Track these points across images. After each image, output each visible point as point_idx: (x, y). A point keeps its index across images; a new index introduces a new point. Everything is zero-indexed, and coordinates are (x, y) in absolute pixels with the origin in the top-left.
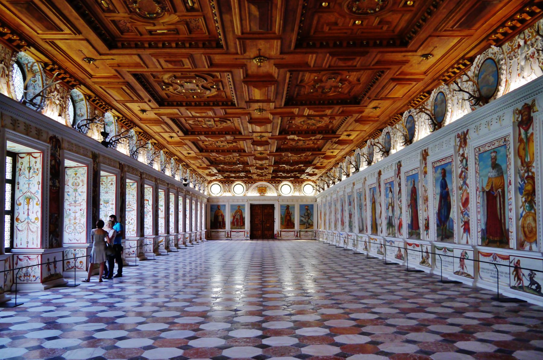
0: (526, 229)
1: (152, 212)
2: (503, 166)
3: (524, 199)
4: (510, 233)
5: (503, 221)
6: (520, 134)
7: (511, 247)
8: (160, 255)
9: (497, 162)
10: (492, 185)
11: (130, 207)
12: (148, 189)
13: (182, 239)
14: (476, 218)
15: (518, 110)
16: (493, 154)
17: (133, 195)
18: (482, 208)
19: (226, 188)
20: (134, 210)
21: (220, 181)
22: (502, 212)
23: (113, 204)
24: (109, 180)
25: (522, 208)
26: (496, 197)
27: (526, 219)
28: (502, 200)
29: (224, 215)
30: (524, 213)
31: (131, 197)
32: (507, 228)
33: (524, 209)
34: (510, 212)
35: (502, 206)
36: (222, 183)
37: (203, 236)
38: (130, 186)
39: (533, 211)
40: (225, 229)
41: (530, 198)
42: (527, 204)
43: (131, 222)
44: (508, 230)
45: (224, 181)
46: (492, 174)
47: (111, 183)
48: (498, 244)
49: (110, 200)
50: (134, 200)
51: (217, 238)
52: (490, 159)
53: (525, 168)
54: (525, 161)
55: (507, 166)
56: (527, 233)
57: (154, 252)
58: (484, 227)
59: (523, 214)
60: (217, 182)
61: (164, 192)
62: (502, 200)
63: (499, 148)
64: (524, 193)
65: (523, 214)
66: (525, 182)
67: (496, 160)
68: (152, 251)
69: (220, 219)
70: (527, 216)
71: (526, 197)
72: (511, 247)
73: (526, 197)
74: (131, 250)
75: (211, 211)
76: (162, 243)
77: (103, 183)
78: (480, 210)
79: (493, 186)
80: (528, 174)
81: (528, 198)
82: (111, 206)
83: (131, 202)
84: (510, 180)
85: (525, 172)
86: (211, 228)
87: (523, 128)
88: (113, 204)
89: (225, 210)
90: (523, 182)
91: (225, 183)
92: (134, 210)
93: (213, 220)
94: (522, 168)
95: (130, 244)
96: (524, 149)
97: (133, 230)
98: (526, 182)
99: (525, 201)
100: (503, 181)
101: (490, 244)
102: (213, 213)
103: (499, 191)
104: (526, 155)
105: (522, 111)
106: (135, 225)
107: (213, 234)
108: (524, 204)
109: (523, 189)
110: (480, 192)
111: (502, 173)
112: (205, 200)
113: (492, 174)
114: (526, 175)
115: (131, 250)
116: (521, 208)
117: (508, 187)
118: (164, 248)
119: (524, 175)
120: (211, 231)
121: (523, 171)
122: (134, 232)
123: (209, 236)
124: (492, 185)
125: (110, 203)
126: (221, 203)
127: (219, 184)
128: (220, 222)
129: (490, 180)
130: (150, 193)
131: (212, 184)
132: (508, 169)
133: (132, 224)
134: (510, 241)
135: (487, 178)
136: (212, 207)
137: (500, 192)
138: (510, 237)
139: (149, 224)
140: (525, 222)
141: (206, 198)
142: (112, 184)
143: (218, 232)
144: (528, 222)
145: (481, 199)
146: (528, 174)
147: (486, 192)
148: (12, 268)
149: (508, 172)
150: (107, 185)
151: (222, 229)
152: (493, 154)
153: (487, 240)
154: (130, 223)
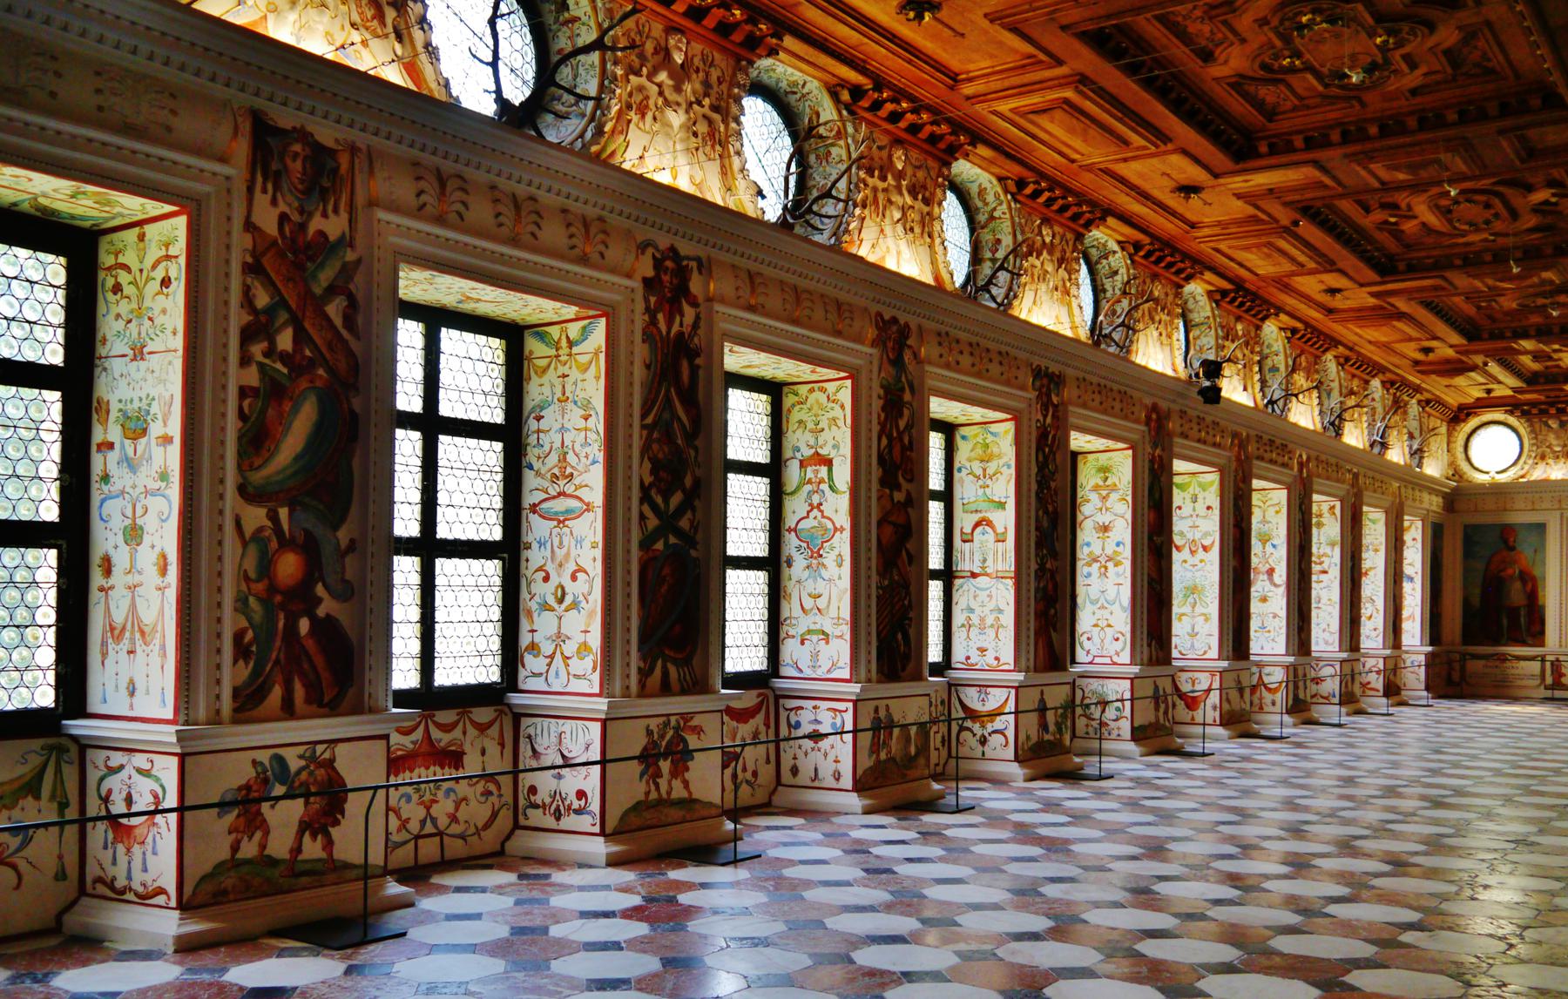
1: (847, 535)
8: (1256, 736)
11: (570, 489)
12: (831, 387)
13: (1214, 698)
17: (587, 405)
19: (1551, 438)
20: (588, 507)
21: (1512, 405)
23: (167, 440)
24: (154, 253)
29: (1537, 572)
31: (574, 417)
36: (1525, 415)
37: (1415, 676)
38: (571, 344)
40: (1542, 644)
43: (570, 587)
45: (1533, 404)
47: (159, 274)
49: (155, 409)
50: (592, 436)
51: (1501, 690)
57: (1387, 694)
60: (1498, 415)
61: (1010, 426)
68: (847, 781)
69: (1516, 595)
74: (572, 782)
75: (1468, 554)
76: (999, 723)
77: (124, 278)
82: (157, 452)
83: (571, 458)
86: (1469, 636)
88: (167, 440)
89: (1540, 548)
91: (1543, 412)
92: (588, 507)
93: (1476, 601)
95: (566, 741)
97: (584, 648)
102: (1480, 565)
106: (591, 614)
107: (1475, 666)
112: (1434, 503)
115: (572, 782)
118: (1010, 753)
120: (1464, 655)
122: (588, 663)
123: (1456, 676)
125: (156, 429)
126: (1520, 517)
127: (1512, 420)
128: (1514, 612)
130: (838, 412)
131: (1474, 422)
133: (575, 605)
136: (1472, 536)
139: (833, 613)
141: (1432, 491)
142: (166, 282)
143: (1503, 658)
148: (72, 813)
150: (141, 298)
151: (1524, 643)
154: (568, 600)
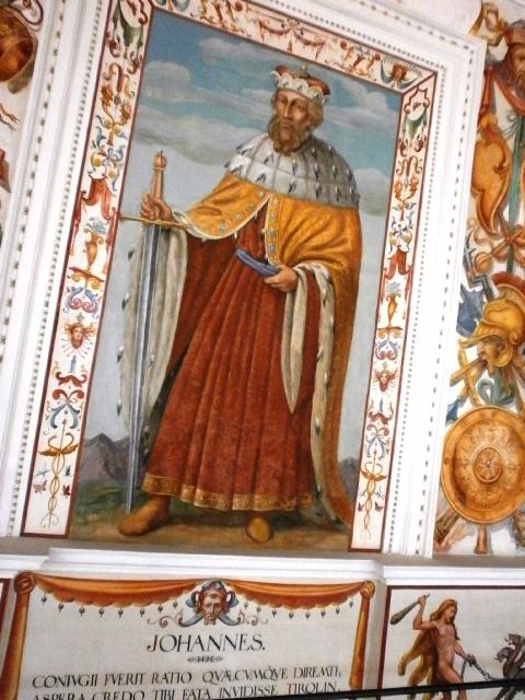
0: (467, 472)
2: (367, 177)
3: (472, 354)
4: (363, 482)
5: (317, 420)
6: (487, 107)
7: (357, 542)
9: (318, 133)
10: (258, 222)
14: (33, 366)
15: (496, 13)
16: (310, 92)
18: (115, 315)
22: (322, 375)
25: (462, 384)
26: (279, 295)
27: (475, 433)
28: (327, 319)
30: (467, 407)
32: (344, 452)
33: (468, 388)
34: (383, 387)
35: (324, 347)
39: (513, 409)
41: (504, 360)
42: (485, 376)
44: (354, 467)
46: (267, 170)
48: (258, 528)
52: (270, 95)
53: (496, 243)
54: (499, 214)
55: (393, 189)
56: (474, 487)
58: (118, 429)
59: (461, 412)
62: (327, 319)
63: (346, 82)
64: (479, 330)
65: (461, 412)
66: (487, 292)
67: (317, 122)
70: (483, 421)
71: (489, 348)
72: (357, 542)
73: (489, 348)
78: (90, 320)
79: (267, 228)
80: (510, 268)
81: (497, 355)
84: (401, 255)
85: (496, 254)
87: (508, 97)
90: (479, 288)
94: (482, 234)
96: (500, 169)
98: (496, 292)
99: (482, 363)
100: (349, 234)
101: (161, 532)
103: (311, 275)
104: (505, 198)
105: (516, 38)
108: (474, 372)
109: (479, 316)
110: (118, 218)
111: (355, 198)
113: (267, 170)
114: (500, 267)
116: (454, 382)
117: (384, 276)
119: (489, 261)
121: (488, 249)
124: (258, 222)
129: (243, 190)
132: (395, 202)
134: (359, 517)
135: (216, 174)
137: (321, 282)
138: (361, 500)
140: (466, 443)
144: (484, 444)
145: (124, 272)
146: (510, 268)
147: (193, 242)
149: (396, 215)
152: (310, 92)
153: (148, 510)
